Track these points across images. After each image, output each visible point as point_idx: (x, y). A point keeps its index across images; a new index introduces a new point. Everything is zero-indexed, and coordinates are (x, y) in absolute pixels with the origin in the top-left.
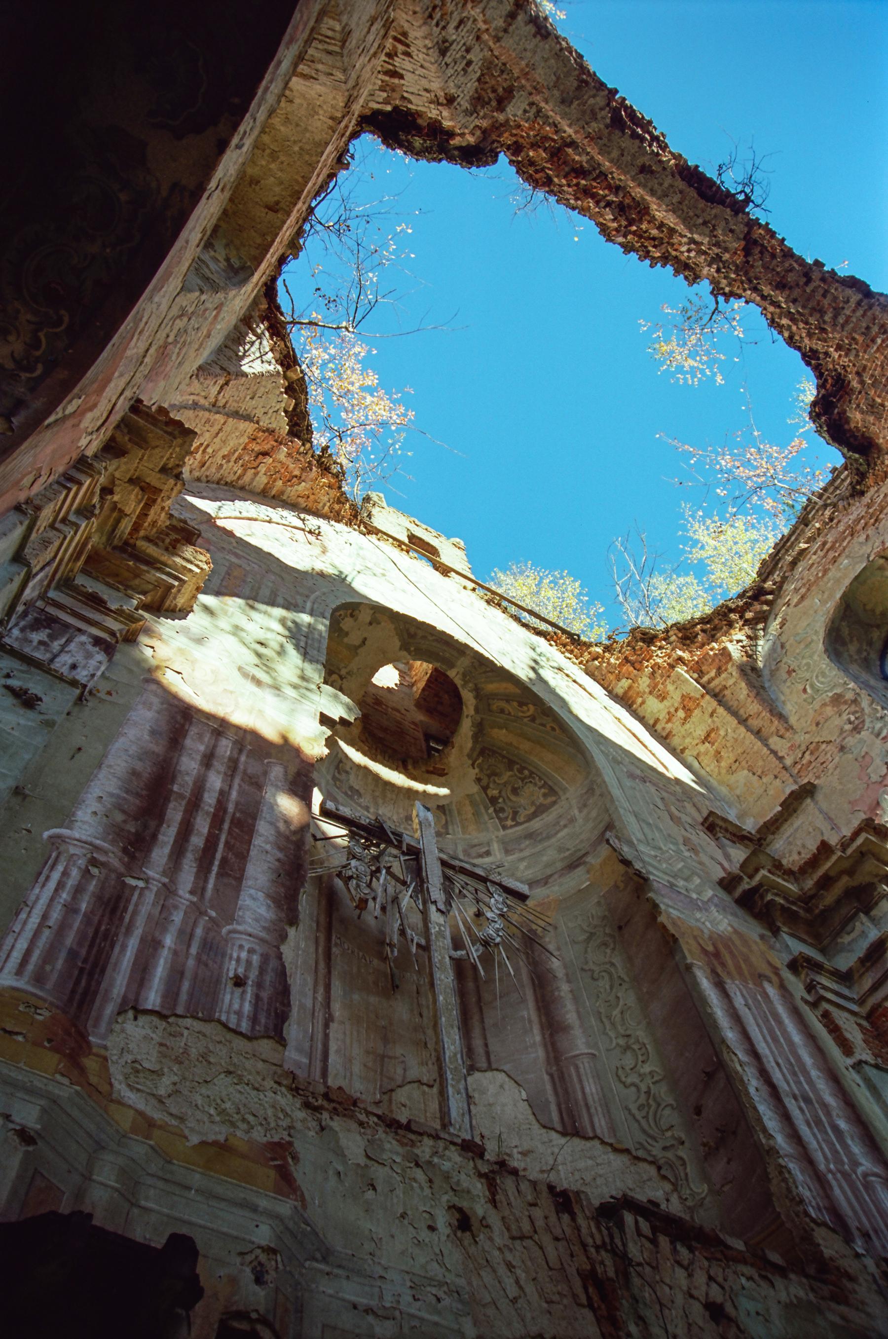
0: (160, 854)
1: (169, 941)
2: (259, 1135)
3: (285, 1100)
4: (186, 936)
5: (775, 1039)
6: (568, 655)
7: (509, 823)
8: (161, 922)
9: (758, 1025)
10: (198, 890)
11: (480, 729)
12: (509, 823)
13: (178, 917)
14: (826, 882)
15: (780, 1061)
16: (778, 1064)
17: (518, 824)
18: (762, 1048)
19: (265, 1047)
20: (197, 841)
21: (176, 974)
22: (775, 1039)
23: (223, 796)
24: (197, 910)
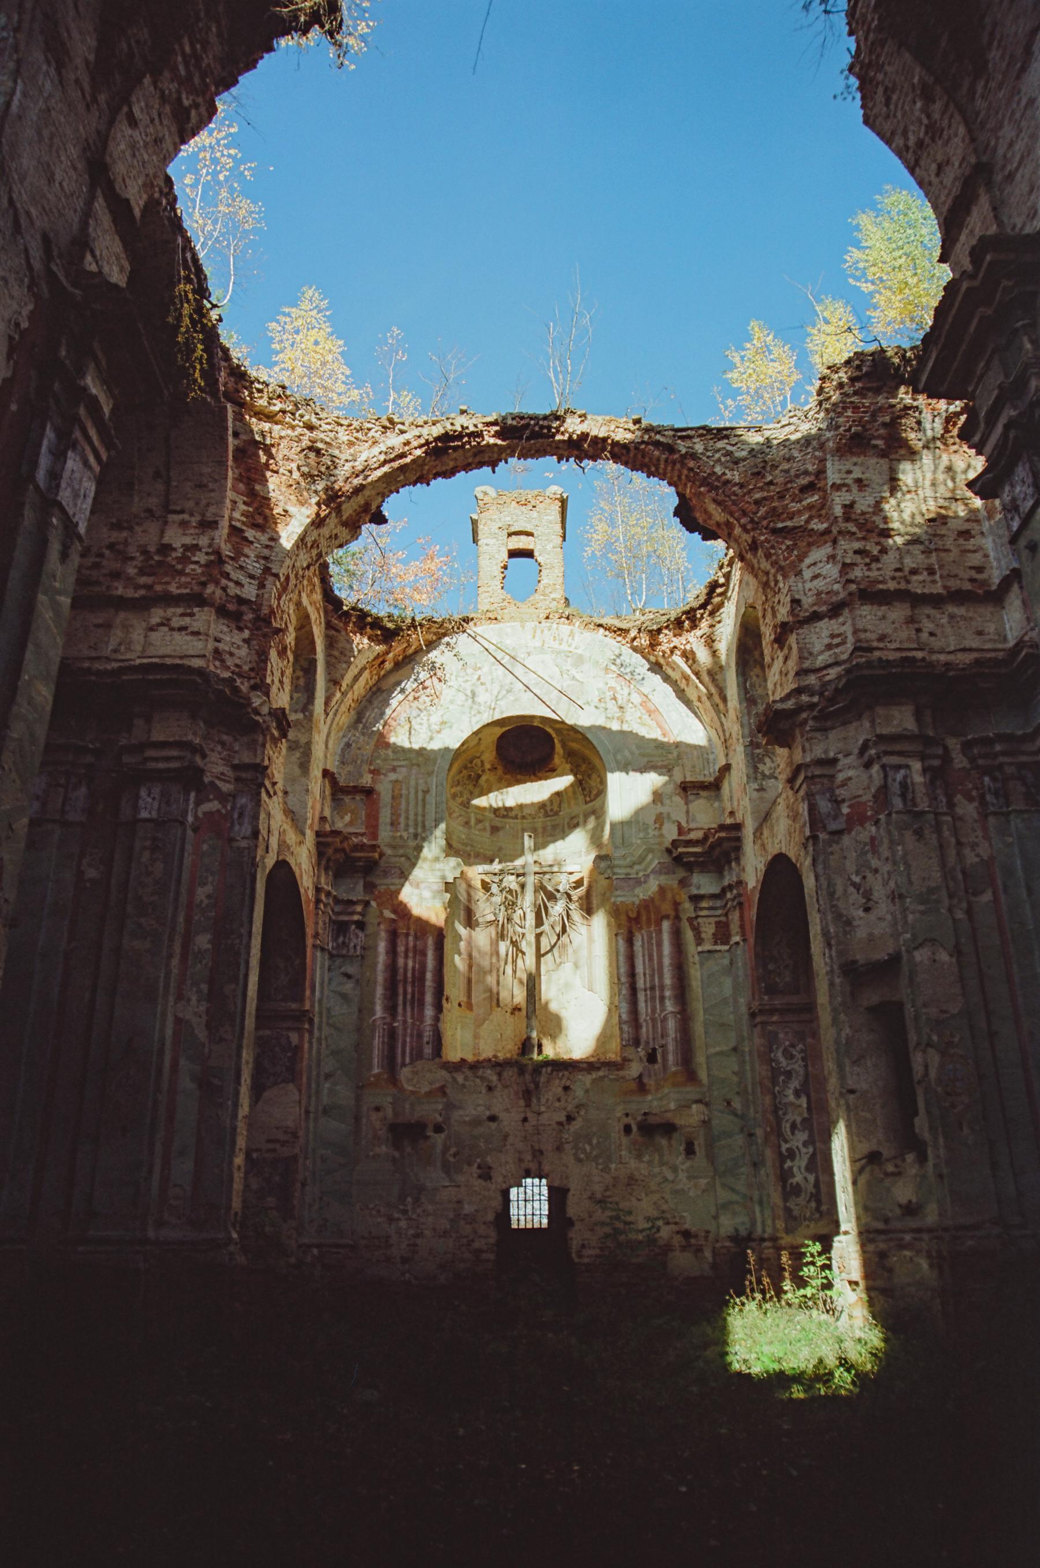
0: (400, 1009)
1: (408, 1040)
2: (438, 1085)
3: (444, 1073)
4: (412, 1036)
5: (651, 959)
6: (619, 639)
7: (588, 799)
8: (405, 1035)
9: (644, 956)
10: (412, 1017)
11: (564, 745)
12: (588, 799)
13: (409, 1031)
15: (647, 972)
16: (645, 974)
17: (591, 801)
18: (639, 969)
19: (437, 1060)
20: (409, 997)
21: (412, 1049)
22: (651, 959)
23: (414, 968)
24: (413, 1024)
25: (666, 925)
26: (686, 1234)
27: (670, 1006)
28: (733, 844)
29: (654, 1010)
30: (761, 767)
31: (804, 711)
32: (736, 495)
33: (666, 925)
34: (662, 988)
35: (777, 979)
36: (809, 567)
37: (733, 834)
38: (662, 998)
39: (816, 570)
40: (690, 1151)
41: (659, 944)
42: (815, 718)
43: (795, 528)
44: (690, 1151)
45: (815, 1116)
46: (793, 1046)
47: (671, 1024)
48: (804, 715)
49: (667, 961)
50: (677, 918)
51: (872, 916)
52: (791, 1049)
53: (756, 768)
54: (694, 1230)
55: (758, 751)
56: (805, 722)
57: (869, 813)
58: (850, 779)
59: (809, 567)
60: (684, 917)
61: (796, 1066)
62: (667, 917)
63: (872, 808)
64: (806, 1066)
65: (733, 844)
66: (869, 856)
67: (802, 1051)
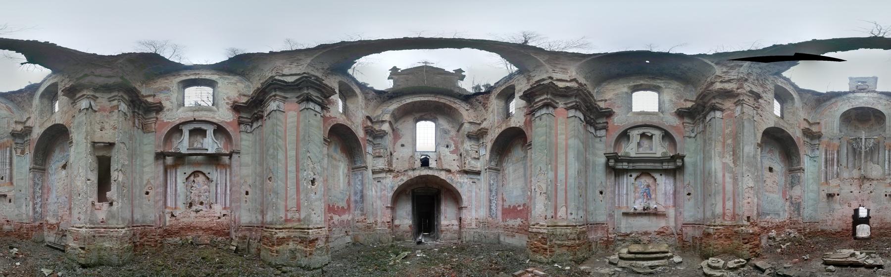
14: (22, 132)
25: (8, 149)
26: (8, 221)
27: (8, 167)
29: (3, 167)
33: (8, 149)
34: (6, 162)
38: (6, 165)
40: (10, 201)
41: (6, 153)
44: (10, 201)
47: (8, 171)
49: (8, 157)
50: (11, 147)
54: (9, 220)
60: (13, 148)
62: (8, 147)
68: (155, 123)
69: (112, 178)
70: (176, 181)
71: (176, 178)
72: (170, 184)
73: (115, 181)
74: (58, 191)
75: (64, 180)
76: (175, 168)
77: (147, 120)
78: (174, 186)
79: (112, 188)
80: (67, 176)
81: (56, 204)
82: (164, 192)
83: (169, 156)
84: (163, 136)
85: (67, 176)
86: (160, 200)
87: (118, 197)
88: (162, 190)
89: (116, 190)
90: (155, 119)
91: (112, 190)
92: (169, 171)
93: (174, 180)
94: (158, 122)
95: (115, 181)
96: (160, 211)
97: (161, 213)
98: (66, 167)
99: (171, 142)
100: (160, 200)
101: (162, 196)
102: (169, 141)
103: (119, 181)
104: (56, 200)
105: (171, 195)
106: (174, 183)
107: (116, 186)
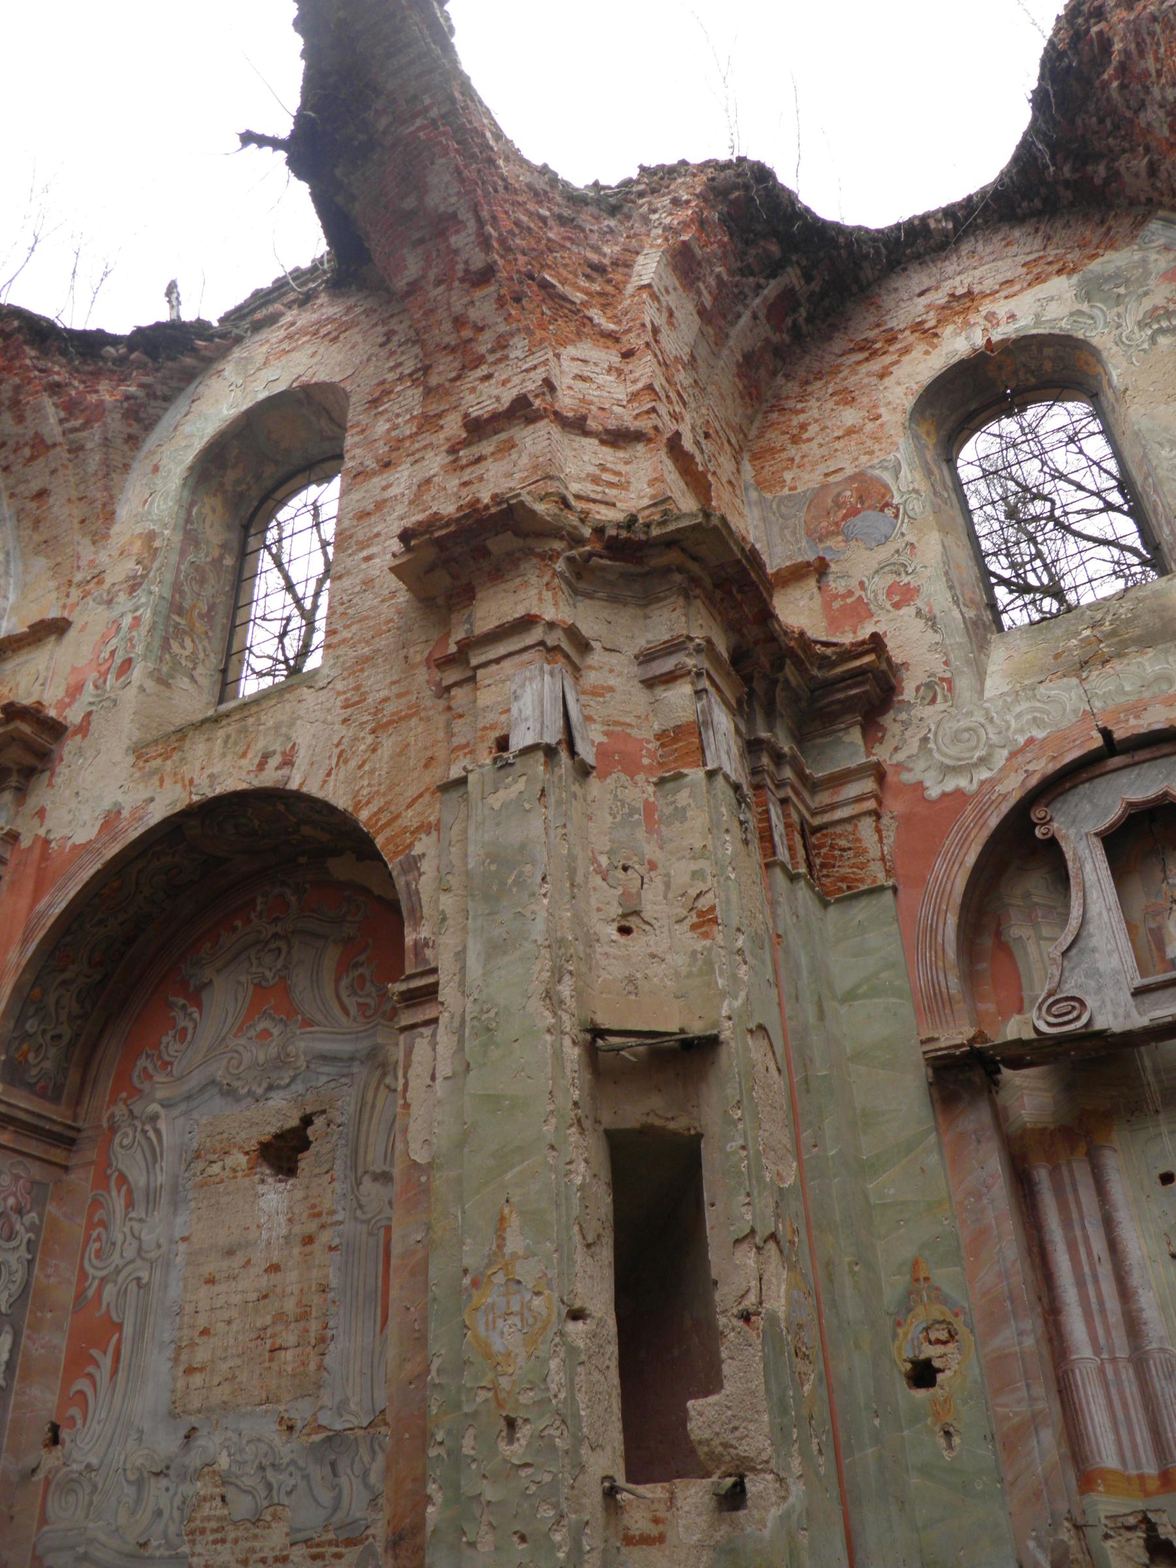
28: (29, 760)
30: (175, 647)
31: (562, 538)
32: (496, 191)
35: (31, 1056)
36: (573, 359)
37: (42, 740)
39: (586, 371)
42: (570, 560)
43: (564, 298)
45: (16, 1385)
46: (19, 1211)
48: (558, 545)
51: (637, 944)
52: (14, 1217)
53: (166, 646)
55: (177, 618)
56: (553, 556)
57: (646, 761)
58: (611, 689)
59: (573, 359)
61: (12, 1259)
63: (651, 754)
64: (30, 1262)
65: (29, 760)
66: (641, 834)
67: (32, 1228)
68: (877, 815)
69: (726, 1297)
70: (1114, 1246)
71: (1109, 1224)
72: (1080, 1283)
73: (746, 1317)
74: (201, 1356)
75: (274, 1268)
76: (1082, 1148)
77: (824, 798)
78: (1108, 1288)
79: (727, 1369)
80: (309, 1240)
81: (156, 1487)
82: (1045, 1352)
83: (1017, 1064)
84: (952, 920)
85: (309, 1240)
86: (1034, 1422)
87: (780, 1435)
88: (1029, 1342)
89: (758, 1383)
90: (868, 785)
91: (728, 1388)
92: (1042, 1176)
93: (1099, 1246)
94: (895, 806)
95: (746, 1317)
96: (1055, 1526)
97: (1066, 1535)
98: (306, 1162)
99: (1004, 948)
100: (1034, 1422)
101: (1039, 1390)
102: (988, 942)
103: (772, 1319)
104: (166, 1443)
105: (1102, 1371)
106: (1105, 1270)
107: (755, 1356)
